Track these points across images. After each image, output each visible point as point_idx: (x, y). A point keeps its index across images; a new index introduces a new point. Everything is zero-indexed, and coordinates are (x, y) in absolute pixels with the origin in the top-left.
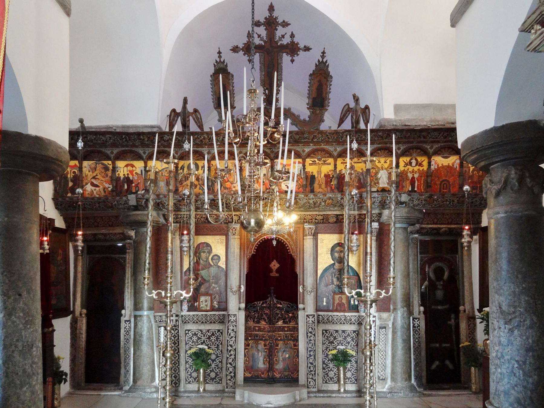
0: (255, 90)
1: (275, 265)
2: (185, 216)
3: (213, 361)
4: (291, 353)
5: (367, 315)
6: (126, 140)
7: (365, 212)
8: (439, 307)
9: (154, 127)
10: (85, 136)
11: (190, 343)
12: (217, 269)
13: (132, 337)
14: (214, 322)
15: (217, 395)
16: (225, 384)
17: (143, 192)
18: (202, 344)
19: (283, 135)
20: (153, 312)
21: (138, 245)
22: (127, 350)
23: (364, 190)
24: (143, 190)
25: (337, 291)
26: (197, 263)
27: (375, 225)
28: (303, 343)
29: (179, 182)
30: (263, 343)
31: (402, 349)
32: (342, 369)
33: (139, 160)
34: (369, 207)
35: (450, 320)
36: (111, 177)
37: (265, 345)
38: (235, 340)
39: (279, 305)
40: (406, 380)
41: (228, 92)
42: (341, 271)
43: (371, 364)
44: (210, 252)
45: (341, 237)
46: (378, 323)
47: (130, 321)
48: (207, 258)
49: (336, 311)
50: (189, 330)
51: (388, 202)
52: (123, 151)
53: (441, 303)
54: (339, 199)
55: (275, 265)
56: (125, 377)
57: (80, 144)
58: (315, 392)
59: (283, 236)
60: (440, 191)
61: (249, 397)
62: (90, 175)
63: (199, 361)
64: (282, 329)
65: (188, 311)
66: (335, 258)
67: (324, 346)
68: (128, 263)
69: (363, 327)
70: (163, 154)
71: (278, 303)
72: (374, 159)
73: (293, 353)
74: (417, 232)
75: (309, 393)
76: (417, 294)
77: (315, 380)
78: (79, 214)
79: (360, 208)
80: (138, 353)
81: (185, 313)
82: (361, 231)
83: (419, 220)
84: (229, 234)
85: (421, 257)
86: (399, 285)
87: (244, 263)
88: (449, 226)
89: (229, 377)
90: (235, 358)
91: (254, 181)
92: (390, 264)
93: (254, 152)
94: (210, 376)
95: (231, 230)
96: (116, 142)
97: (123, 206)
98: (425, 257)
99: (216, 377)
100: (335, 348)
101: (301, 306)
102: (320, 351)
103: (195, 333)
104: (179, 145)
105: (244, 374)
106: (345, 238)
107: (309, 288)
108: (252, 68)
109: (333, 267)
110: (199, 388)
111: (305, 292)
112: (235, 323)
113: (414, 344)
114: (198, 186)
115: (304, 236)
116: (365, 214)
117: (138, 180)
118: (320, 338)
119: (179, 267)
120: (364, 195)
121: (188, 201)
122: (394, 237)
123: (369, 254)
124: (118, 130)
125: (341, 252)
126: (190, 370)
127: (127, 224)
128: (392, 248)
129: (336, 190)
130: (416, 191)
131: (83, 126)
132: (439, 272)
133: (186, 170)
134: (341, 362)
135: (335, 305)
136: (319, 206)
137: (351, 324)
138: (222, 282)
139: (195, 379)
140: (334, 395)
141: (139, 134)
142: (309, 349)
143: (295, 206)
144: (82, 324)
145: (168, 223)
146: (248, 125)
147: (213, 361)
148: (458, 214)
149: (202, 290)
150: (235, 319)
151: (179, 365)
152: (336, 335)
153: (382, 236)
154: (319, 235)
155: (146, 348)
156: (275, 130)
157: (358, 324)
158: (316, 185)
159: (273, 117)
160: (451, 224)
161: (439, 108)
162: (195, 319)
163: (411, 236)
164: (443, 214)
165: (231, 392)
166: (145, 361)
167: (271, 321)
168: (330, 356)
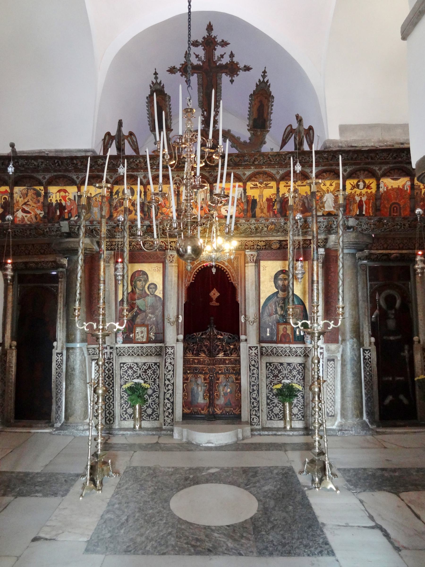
0: (192, 110)
1: (215, 294)
2: (120, 243)
3: (150, 396)
4: (232, 388)
6: (59, 165)
7: (310, 238)
8: (392, 338)
10: (16, 160)
11: (125, 377)
12: (154, 298)
13: (64, 370)
14: (151, 355)
15: (154, 433)
16: (162, 420)
17: (76, 218)
18: (138, 378)
19: (221, 156)
20: (87, 344)
21: (71, 273)
22: (58, 385)
24: (76, 216)
25: (281, 321)
26: (133, 292)
27: (322, 251)
28: (246, 376)
29: (113, 208)
30: (203, 377)
31: (353, 383)
32: (287, 404)
33: (72, 185)
34: (315, 233)
35: (404, 352)
36: (43, 203)
37: (205, 379)
38: (173, 374)
39: (220, 337)
40: (357, 418)
41: (164, 112)
42: (285, 300)
43: (320, 401)
44: (146, 280)
46: (326, 355)
47: (61, 353)
49: (281, 342)
52: (56, 176)
54: (282, 224)
55: (215, 294)
56: (57, 412)
57: (11, 170)
58: (259, 430)
59: (224, 264)
60: (390, 214)
61: (188, 435)
62: (21, 201)
63: (133, 397)
64: (223, 362)
65: (124, 342)
67: (268, 380)
69: (310, 359)
70: (95, 179)
71: (218, 334)
73: (234, 388)
74: (367, 258)
75: (252, 430)
76: (367, 324)
77: (259, 417)
78: (9, 241)
79: (305, 233)
80: (70, 388)
81: (120, 345)
83: (368, 245)
84: (167, 261)
85: (371, 285)
86: (347, 315)
87: (182, 291)
88: (400, 252)
89: (167, 414)
90: (173, 393)
91: (191, 205)
92: (339, 292)
93: (190, 174)
94: (146, 412)
96: (48, 166)
98: (375, 285)
99: (153, 413)
100: (280, 382)
101: (243, 337)
103: (130, 366)
104: (113, 169)
105: (183, 410)
106: (289, 265)
107: (251, 319)
109: (277, 296)
111: (247, 322)
112: (172, 356)
113: (365, 377)
114: (134, 212)
115: (245, 263)
116: (310, 240)
117: (71, 206)
118: (263, 371)
119: (113, 297)
120: (310, 219)
121: (123, 227)
122: (343, 264)
123: (315, 282)
124: (51, 155)
125: (285, 279)
126: (125, 406)
127: (60, 252)
128: (341, 276)
129: (279, 215)
130: (364, 215)
131: (14, 151)
133: (120, 194)
134: (287, 397)
135: (280, 336)
136: (261, 232)
137: (296, 356)
138: (159, 312)
139: (130, 416)
140: (279, 433)
142: (252, 383)
143: (236, 232)
144: (12, 357)
145: (100, 251)
146: (184, 146)
147: (150, 396)
148: (410, 238)
150: (172, 351)
151: (113, 401)
152: (280, 368)
153: (329, 262)
154: (261, 262)
155: (78, 382)
156: (213, 151)
157: (305, 356)
158: (258, 210)
159: (210, 137)
160: (402, 249)
161: (387, 128)
162: (131, 351)
163: (360, 263)
164: (394, 239)
166: (77, 397)
167: (211, 353)
168: (275, 391)
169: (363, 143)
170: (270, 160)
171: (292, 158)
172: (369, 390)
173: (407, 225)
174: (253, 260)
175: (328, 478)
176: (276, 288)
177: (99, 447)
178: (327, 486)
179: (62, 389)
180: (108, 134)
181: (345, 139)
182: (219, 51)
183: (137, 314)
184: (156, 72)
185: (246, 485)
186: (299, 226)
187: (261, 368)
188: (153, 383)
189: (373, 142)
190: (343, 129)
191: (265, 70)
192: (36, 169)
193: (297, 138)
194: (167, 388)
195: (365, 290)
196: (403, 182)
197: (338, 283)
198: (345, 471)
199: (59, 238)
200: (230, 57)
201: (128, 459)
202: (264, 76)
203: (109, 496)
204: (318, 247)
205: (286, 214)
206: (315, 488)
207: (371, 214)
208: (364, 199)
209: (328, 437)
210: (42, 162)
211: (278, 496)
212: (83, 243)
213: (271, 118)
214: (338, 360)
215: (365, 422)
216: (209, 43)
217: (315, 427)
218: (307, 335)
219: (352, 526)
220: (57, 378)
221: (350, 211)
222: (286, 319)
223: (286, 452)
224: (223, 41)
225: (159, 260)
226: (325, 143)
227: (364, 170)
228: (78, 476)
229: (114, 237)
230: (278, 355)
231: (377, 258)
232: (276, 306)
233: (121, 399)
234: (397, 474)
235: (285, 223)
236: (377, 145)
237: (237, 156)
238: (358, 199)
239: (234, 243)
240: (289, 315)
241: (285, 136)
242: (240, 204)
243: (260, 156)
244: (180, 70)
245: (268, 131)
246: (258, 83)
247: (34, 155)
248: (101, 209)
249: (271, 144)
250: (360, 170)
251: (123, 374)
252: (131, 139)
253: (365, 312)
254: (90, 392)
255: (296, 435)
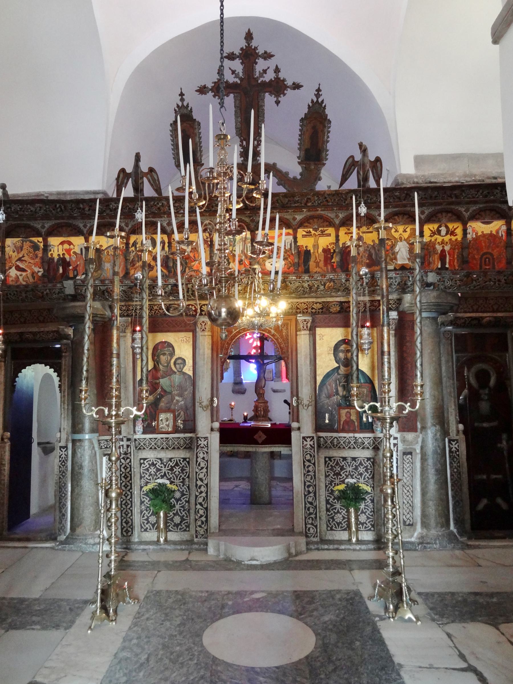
2: (138, 307)
3: (178, 500)
5: (386, 438)
7: (379, 298)
8: (485, 425)
9: (98, 193)
13: (70, 468)
14: (178, 448)
15: (184, 547)
16: (193, 532)
17: (84, 276)
18: (162, 477)
20: (97, 434)
23: (376, 268)
24: (83, 274)
27: (394, 315)
28: (299, 474)
32: (352, 510)
35: (501, 443)
36: (42, 258)
38: (207, 472)
40: (442, 527)
42: (348, 378)
45: (347, 332)
46: (401, 447)
47: (66, 447)
48: (169, 363)
49: (343, 431)
50: (145, 459)
51: (409, 284)
52: (58, 224)
53: (487, 419)
54: (344, 281)
56: (60, 523)
58: (317, 543)
59: (269, 332)
61: (226, 550)
63: (157, 502)
65: (144, 433)
66: (340, 359)
67: (328, 479)
68: (65, 370)
69: (381, 453)
72: (391, 225)
75: (308, 544)
76: (453, 407)
77: (316, 527)
79: (372, 293)
80: (76, 491)
81: (139, 436)
82: (375, 323)
84: (197, 330)
86: (427, 395)
87: (217, 368)
88: (495, 315)
89: (199, 523)
90: (207, 496)
92: (416, 366)
94: (173, 521)
95: (199, 326)
96: (48, 212)
97: (57, 296)
99: (181, 522)
100: (343, 482)
102: (323, 485)
103: (153, 463)
104: (129, 214)
108: (221, 107)
110: (158, 538)
111: (300, 407)
112: (206, 449)
113: (452, 475)
115: (296, 331)
116: (379, 301)
117: (76, 261)
118: (322, 468)
120: (378, 274)
122: (421, 330)
123: (386, 353)
124: (51, 198)
126: (147, 513)
128: (419, 345)
129: (339, 270)
130: (447, 269)
131: (5, 193)
132: (482, 377)
135: (342, 423)
136: (316, 291)
137: (363, 448)
138: (188, 393)
139: (153, 525)
140: (343, 547)
141: (78, 202)
142: (308, 484)
143: (284, 291)
144: (5, 452)
147: (178, 500)
148: (507, 298)
149: (162, 404)
150: (205, 443)
151: (131, 506)
152: (343, 463)
153: (404, 328)
154: (317, 329)
155: (87, 484)
157: (374, 448)
158: (312, 263)
160: (498, 311)
162: (153, 444)
163: (443, 329)
164: (486, 299)
165: (202, 544)
169: (445, 178)
170: (327, 201)
171: (354, 197)
172: (457, 491)
173: (503, 281)
174: (307, 327)
175: (405, 606)
176: (336, 362)
177: (113, 566)
178: (405, 615)
179: (67, 491)
180: (123, 170)
181: (423, 174)
182: (261, 65)
183: (162, 396)
184: (181, 92)
185: (301, 614)
186: (365, 283)
187: (319, 464)
188: (182, 484)
189: (458, 176)
190: (419, 160)
191: (319, 88)
192: (33, 217)
193: (361, 173)
194: (199, 490)
195: (450, 364)
196: (497, 226)
197: (416, 354)
198: (426, 596)
199: (61, 301)
200: (275, 72)
201: (150, 580)
202: (318, 96)
203: (126, 628)
204: (389, 309)
205: (348, 268)
206: (389, 618)
207: (457, 268)
208: (447, 248)
209: (406, 553)
210: (40, 207)
211: (341, 628)
212: (90, 307)
213: (328, 148)
214: (417, 454)
215: (452, 532)
216: (249, 55)
217: (388, 539)
218: (377, 422)
219: (437, 668)
220: (60, 478)
221: (429, 263)
222: (349, 401)
223: (352, 572)
224: (266, 52)
225: (188, 327)
226: (396, 180)
227: (447, 212)
228: (86, 602)
229: (131, 300)
230: (339, 447)
231: (464, 323)
232: (336, 385)
233: (141, 504)
234: (495, 600)
235: (347, 280)
236: (463, 180)
237: (285, 195)
238: (439, 248)
239: (283, 305)
240: (353, 396)
241: (346, 170)
242: (289, 256)
243: (314, 195)
244: (212, 90)
245: (324, 164)
246: (311, 104)
247: (30, 198)
248: (114, 265)
249: (328, 180)
250: (441, 212)
251: (143, 473)
252: (152, 176)
253: (450, 392)
254: (101, 495)
255: (364, 550)
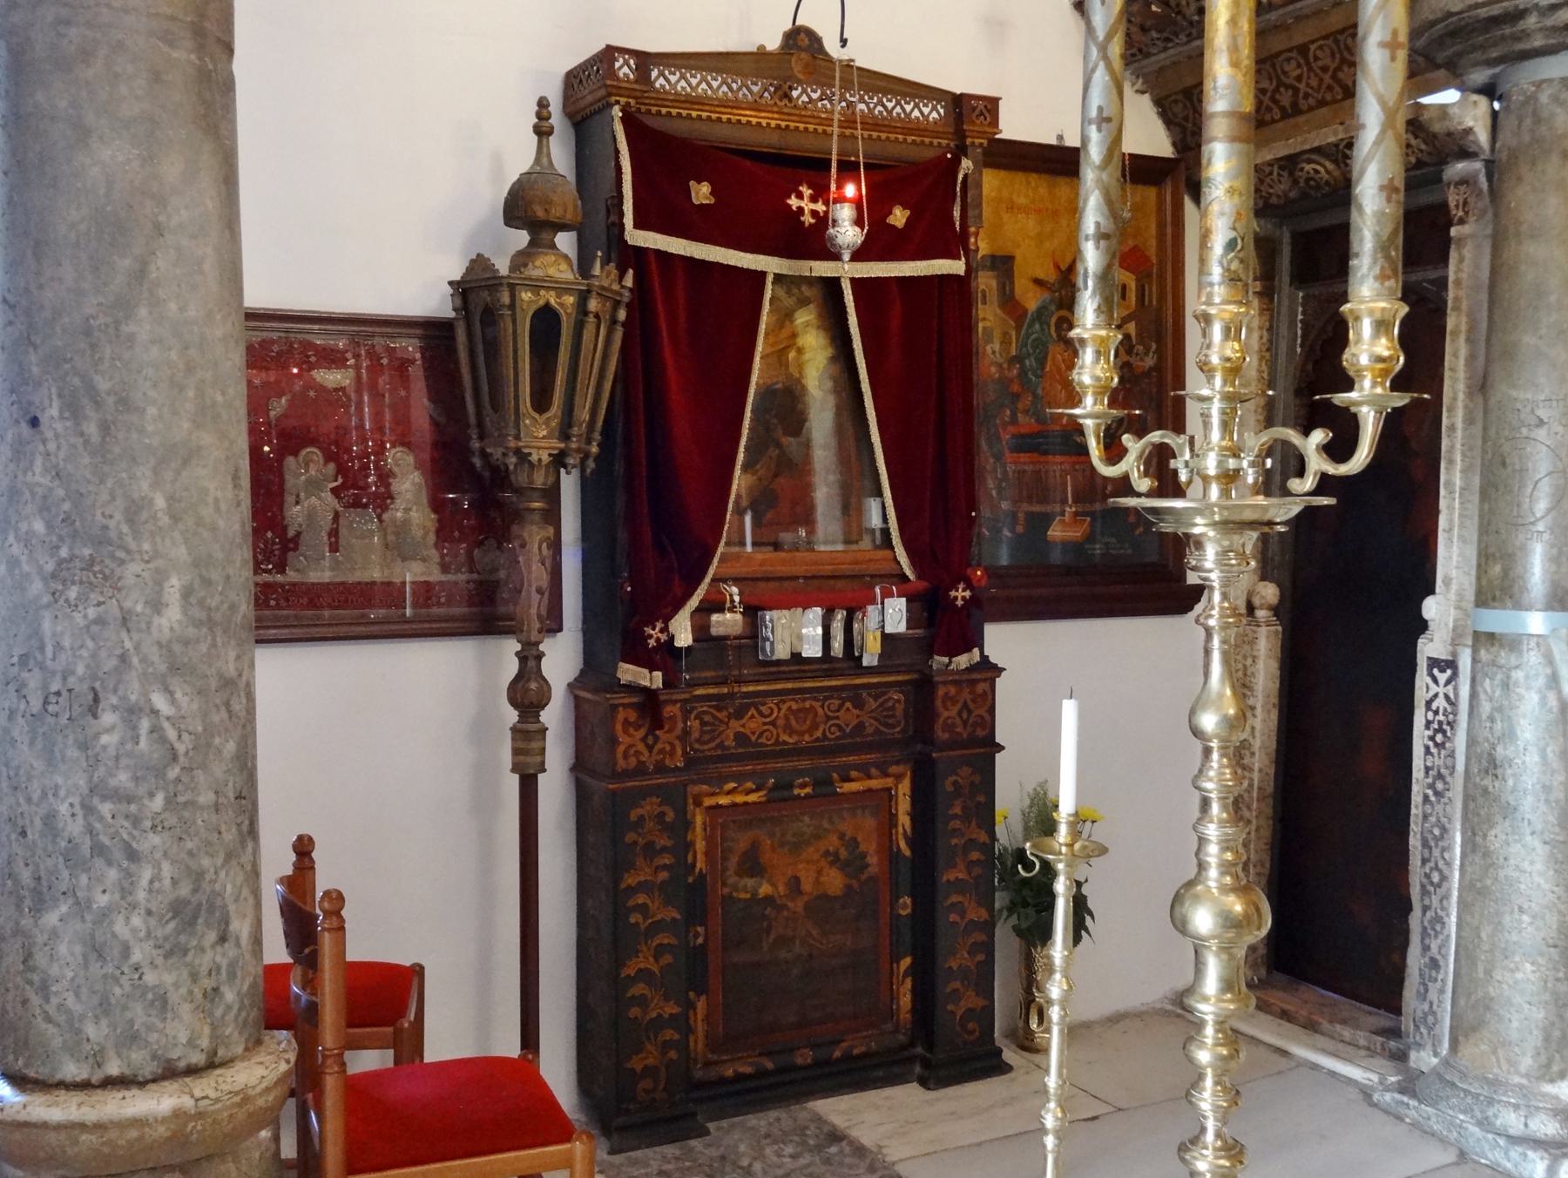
47: (1451, 664)
